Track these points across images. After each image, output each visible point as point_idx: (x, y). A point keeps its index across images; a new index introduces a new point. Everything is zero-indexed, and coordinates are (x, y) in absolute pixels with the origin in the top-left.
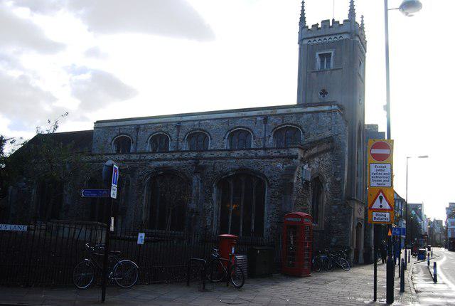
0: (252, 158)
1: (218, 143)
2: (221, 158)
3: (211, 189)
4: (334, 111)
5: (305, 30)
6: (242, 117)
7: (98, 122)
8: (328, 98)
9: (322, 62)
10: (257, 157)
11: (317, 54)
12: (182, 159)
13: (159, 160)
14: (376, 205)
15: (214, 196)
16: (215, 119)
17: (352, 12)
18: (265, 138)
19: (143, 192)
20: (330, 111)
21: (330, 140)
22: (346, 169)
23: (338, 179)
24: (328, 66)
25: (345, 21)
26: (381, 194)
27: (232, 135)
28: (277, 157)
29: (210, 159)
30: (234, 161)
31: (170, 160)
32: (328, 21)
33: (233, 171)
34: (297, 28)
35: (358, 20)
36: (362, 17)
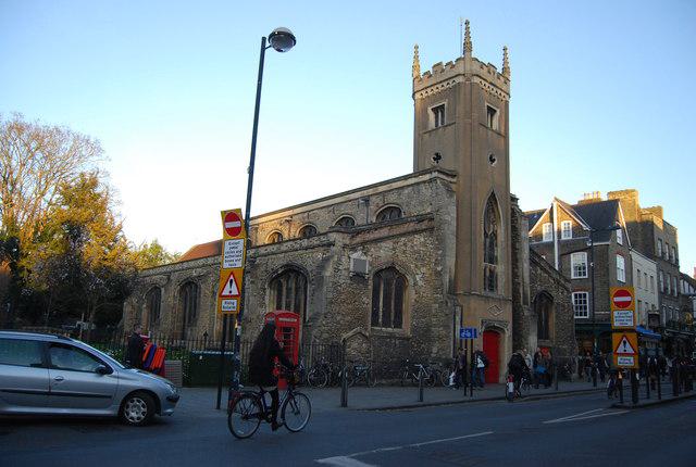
2: (273, 254)
4: (435, 179)
9: (437, 117)
11: (430, 109)
14: (226, 293)
17: (467, 47)
20: (430, 181)
21: (420, 219)
23: (439, 269)
26: (232, 278)
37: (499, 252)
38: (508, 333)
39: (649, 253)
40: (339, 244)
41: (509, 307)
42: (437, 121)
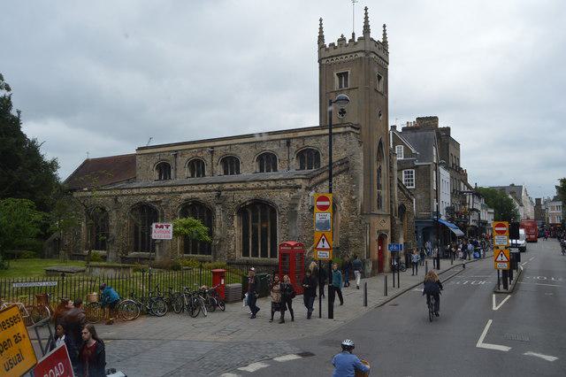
0: (264, 189)
2: (238, 189)
4: (349, 132)
5: (323, 50)
7: (139, 149)
10: (268, 187)
13: (187, 192)
14: (320, 246)
16: (241, 144)
17: (367, 29)
20: (345, 133)
22: (361, 187)
23: (354, 197)
24: (346, 85)
28: (286, 187)
29: (231, 190)
31: (197, 191)
34: (316, 47)
37: (382, 182)
38: (389, 238)
39: (447, 168)
40: (303, 187)
41: (389, 220)
42: (341, 84)
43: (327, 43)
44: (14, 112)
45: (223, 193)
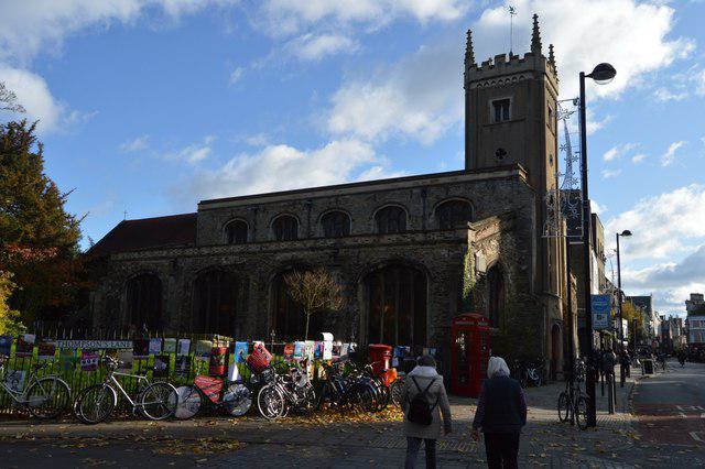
0: (407, 244)
1: (362, 224)
2: (366, 246)
3: (356, 286)
6: (393, 190)
7: (202, 203)
8: (507, 160)
9: (497, 110)
11: (491, 101)
12: (317, 249)
13: (286, 250)
15: (360, 297)
18: (424, 217)
19: (267, 293)
22: (534, 253)
23: (524, 268)
25: (526, 55)
27: (379, 215)
28: (444, 241)
29: (354, 247)
30: (382, 249)
31: (301, 250)
32: (504, 56)
33: (382, 262)
34: (463, 69)
35: (545, 52)
36: (551, 47)
43: (479, 61)
44: (33, 150)
45: (342, 252)
